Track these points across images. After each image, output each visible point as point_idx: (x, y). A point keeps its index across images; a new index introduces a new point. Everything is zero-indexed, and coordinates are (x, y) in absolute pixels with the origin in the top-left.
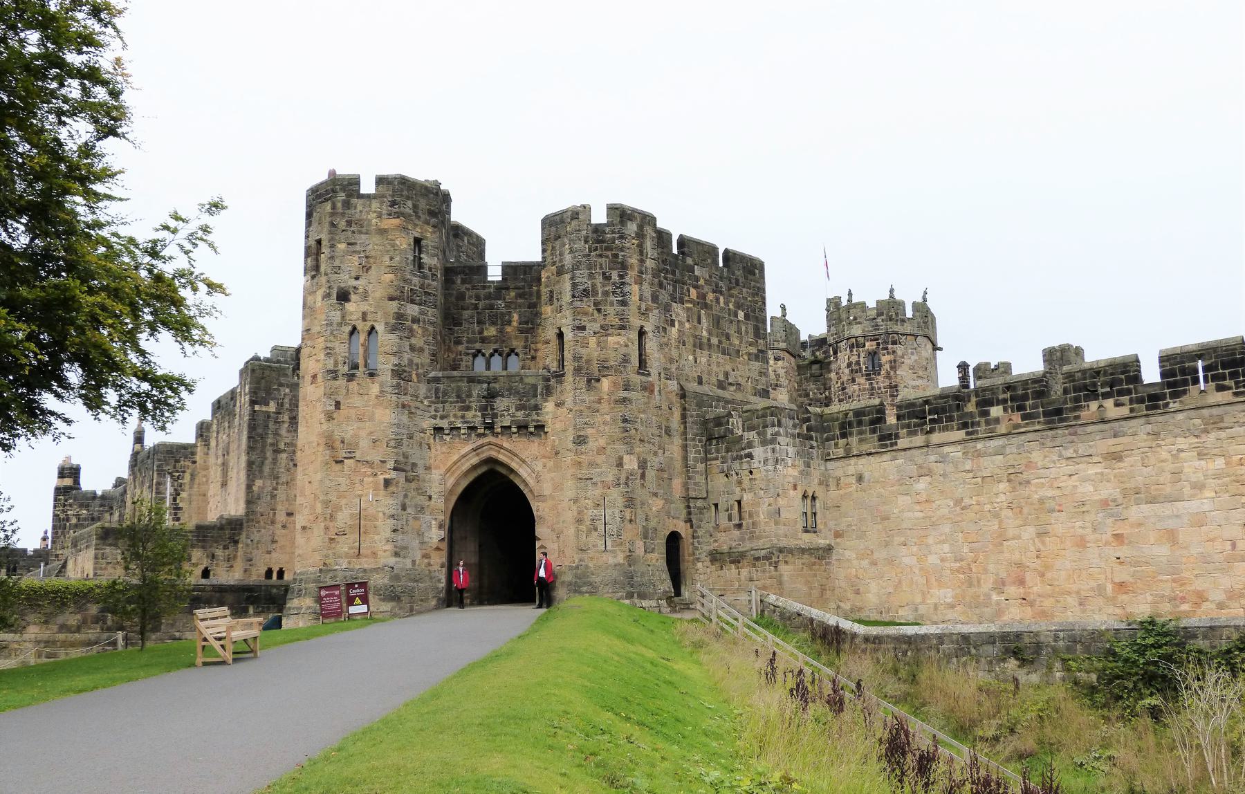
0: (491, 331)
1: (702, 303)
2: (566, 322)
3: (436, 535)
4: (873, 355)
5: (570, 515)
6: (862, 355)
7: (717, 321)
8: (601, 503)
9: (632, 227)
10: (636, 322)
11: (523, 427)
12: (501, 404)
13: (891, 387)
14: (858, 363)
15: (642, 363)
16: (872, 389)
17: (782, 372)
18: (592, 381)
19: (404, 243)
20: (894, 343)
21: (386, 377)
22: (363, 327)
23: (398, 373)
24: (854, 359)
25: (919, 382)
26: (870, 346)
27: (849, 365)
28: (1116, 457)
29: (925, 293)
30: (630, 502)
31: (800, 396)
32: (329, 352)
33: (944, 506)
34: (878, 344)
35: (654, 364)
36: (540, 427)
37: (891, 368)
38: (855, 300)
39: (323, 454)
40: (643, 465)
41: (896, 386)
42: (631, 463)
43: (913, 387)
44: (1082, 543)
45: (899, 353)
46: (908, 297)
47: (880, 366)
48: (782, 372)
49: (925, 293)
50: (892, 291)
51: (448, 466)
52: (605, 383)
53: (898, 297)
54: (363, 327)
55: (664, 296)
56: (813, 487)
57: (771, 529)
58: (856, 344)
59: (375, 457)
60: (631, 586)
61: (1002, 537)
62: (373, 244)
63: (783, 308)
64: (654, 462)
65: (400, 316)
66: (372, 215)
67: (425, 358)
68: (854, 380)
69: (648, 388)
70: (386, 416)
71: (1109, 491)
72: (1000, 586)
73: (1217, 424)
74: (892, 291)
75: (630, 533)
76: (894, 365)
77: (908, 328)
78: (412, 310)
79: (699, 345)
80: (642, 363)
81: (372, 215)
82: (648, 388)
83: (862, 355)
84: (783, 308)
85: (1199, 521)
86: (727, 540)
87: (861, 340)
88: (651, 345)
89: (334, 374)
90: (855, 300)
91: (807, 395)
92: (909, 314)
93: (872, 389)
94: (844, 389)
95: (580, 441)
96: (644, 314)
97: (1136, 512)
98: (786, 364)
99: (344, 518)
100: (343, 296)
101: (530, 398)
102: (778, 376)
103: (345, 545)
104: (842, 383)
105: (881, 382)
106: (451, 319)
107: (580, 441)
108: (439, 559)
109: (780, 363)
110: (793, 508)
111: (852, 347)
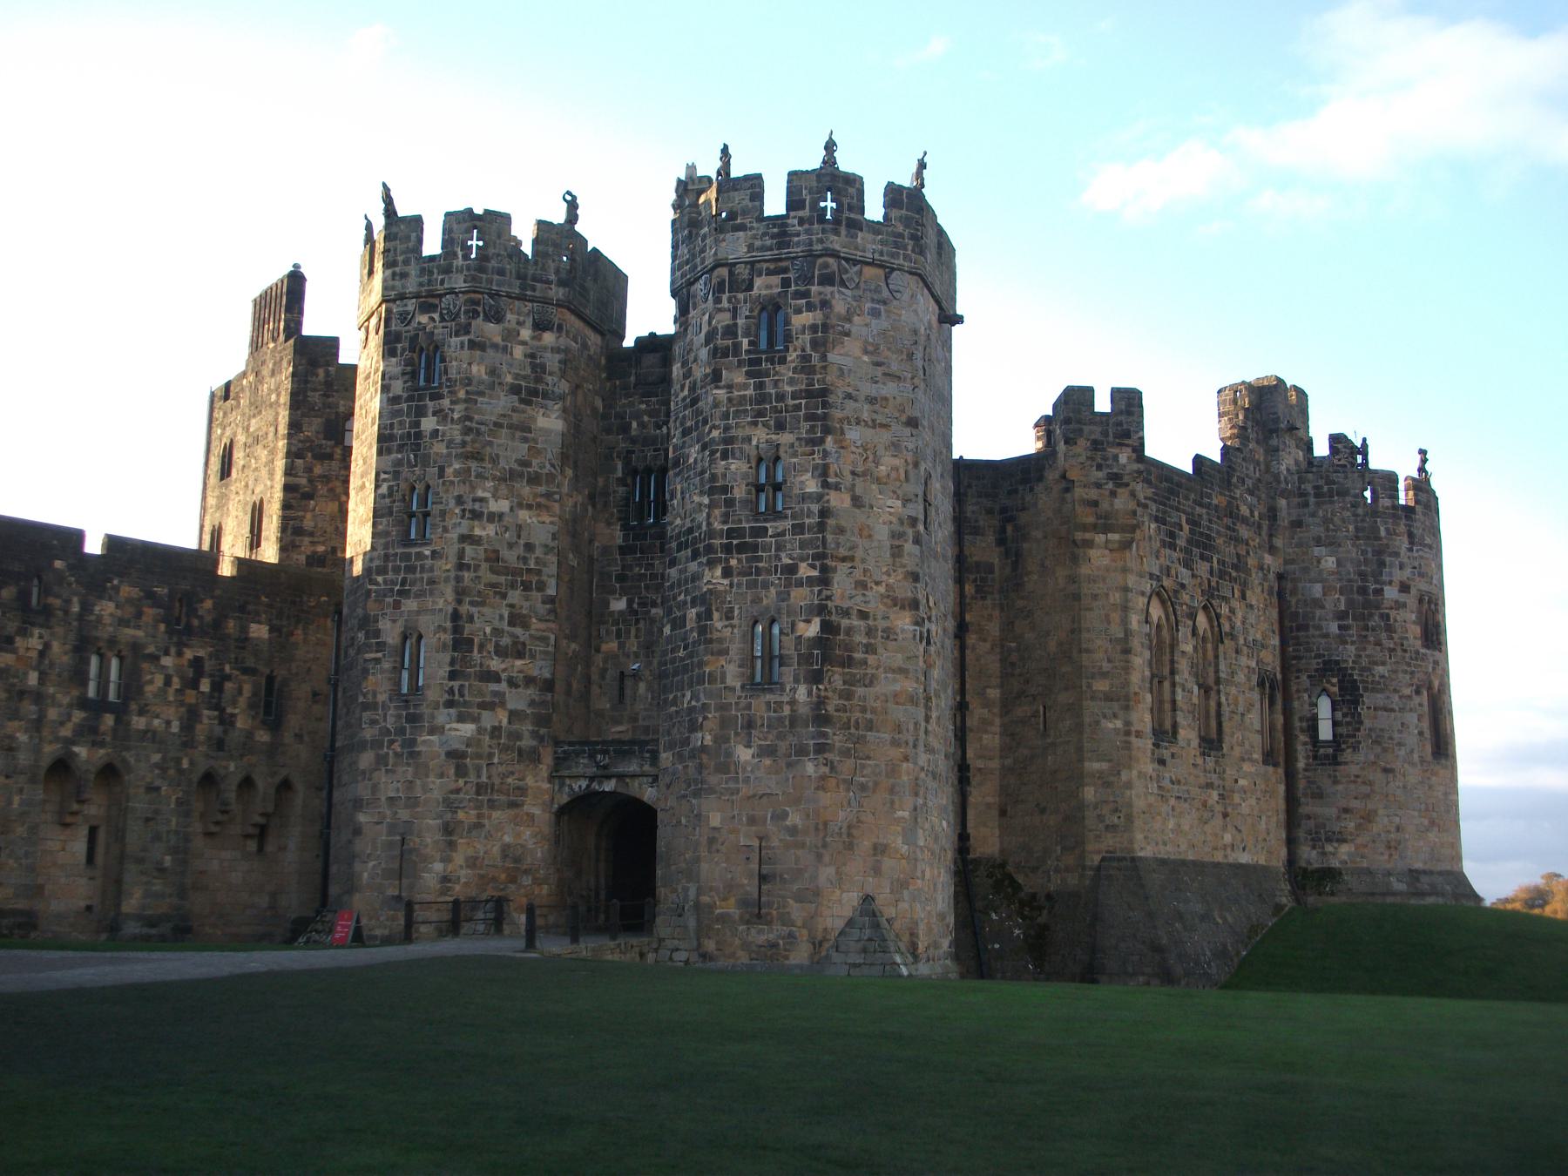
4: (772, 309)
6: (745, 311)
13: (809, 394)
14: (730, 331)
16: (762, 398)
17: (552, 361)
20: (827, 280)
24: (724, 319)
25: (889, 389)
26: (764, 286)
27: (710, 338)
29: (922, 165)
31: (608, 431)
34: (786, 283)
37: (815, 344)
38: (736, 172)
41: (824, 393)
43: (872, 400)
45: (839, 307)
46: (877, 170)
47: (788, 338)
48: (552, 361)
49: (922, 165)
50: (830, 146)
53: (845, 164)
63: (572, 206)
68: (716, 377)
74: (830, 146)
76: (823, 336)
77: (868, 245)
83: (745, 311)
84: (572, 206)
87: (743, 272)
90: (736, 172)
91: (625, 429)
92: (874, 209)
93: (762, 398)
94: (695, 401)
98: (564, 341)
102: (539, 370)
104: (693, 388)
105: (787, 379)
109: (548, 338)
111: (720, 288)
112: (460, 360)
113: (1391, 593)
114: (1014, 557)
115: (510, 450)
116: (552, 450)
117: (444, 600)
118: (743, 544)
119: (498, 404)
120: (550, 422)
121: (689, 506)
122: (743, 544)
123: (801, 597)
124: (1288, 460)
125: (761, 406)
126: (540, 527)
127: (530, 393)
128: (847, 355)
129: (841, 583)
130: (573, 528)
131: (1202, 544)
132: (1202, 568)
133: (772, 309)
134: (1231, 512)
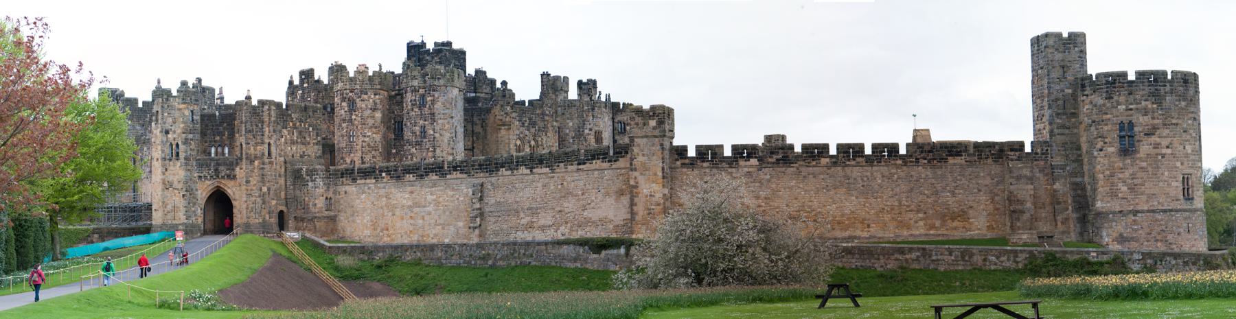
0: (218, 138)
1: (295, 127)
2: (243, 140)
3: (199, 212)
4: (423, 96)
5: (244, 206)
7: (300, 133)
8: (255, 202)
9: (266, 107)
10: (267, 141)
11: (229, 176)
12: (221, 168)
15: (269, 154)
18: (252, 162)
19: (187, 113)
21: (182, 160)
22: (174, 143)
23: (186, 159)
28: (412, 192)
30: (264, 203)
32: (163, 151)
33: (368, 204)
35: (274, 155)
36: (235, 176)
39: (161, 187)
40: (269, 189)
42: (265, 189)
44: (402, 219)
51: (203, 191)
52: (256, 163)
54: (174, 143)
55: (279, 127)
56: (330, 195)
57: (313, 210)
58: (415, 90)
59: (180, 186)
60: (264, 229)
61: (383, 215)
62: (177, 114)
64: (273, 188)
65: (186, 139)
66: (176, 103)
67: (194, 153)
69: (271, 163)
70: (181, 174)
71: (410, 203)
72: (382, 231)
73: (434, 185)
75: (264, 212)
76: (433, 102)
78: (190, 136)
79: (293, 143)
80: (269, 154)
81: (176, 103)
82: (271, 163)
85: (430, 213)
86: (300, 213)
88: (273, 149)
89: (164, 159)
95: (248, 182)
96: (270, 138)
97: (416, 210)
99: (169, 207)
100: (167, 132)
101: (232, 164)
103: (170, 216)
105: (426, 111)
106: (203, 134)
107: (248, 182)
108: (200, 220)
110: (321, 203)
112: (359, 104)
113: (587, 131)
114: (485, 131)
115: (370, 122)
116: (379, 121)
117: (359, 154)
118: (419, 144)
119: (368, 112)
120: (378, 115)
121: (407, 135)
122: (419, 144)
123: (430, 154)
124: (561, 98)
125: (421, 116)
126: (378, 137)
127: (374, 109)
128: (438, 106)
129: (438, 151)
130: (384, 137)
131: (533, 124)
132: (533, 130)
133: (423, 96)
134: (543, 114)
